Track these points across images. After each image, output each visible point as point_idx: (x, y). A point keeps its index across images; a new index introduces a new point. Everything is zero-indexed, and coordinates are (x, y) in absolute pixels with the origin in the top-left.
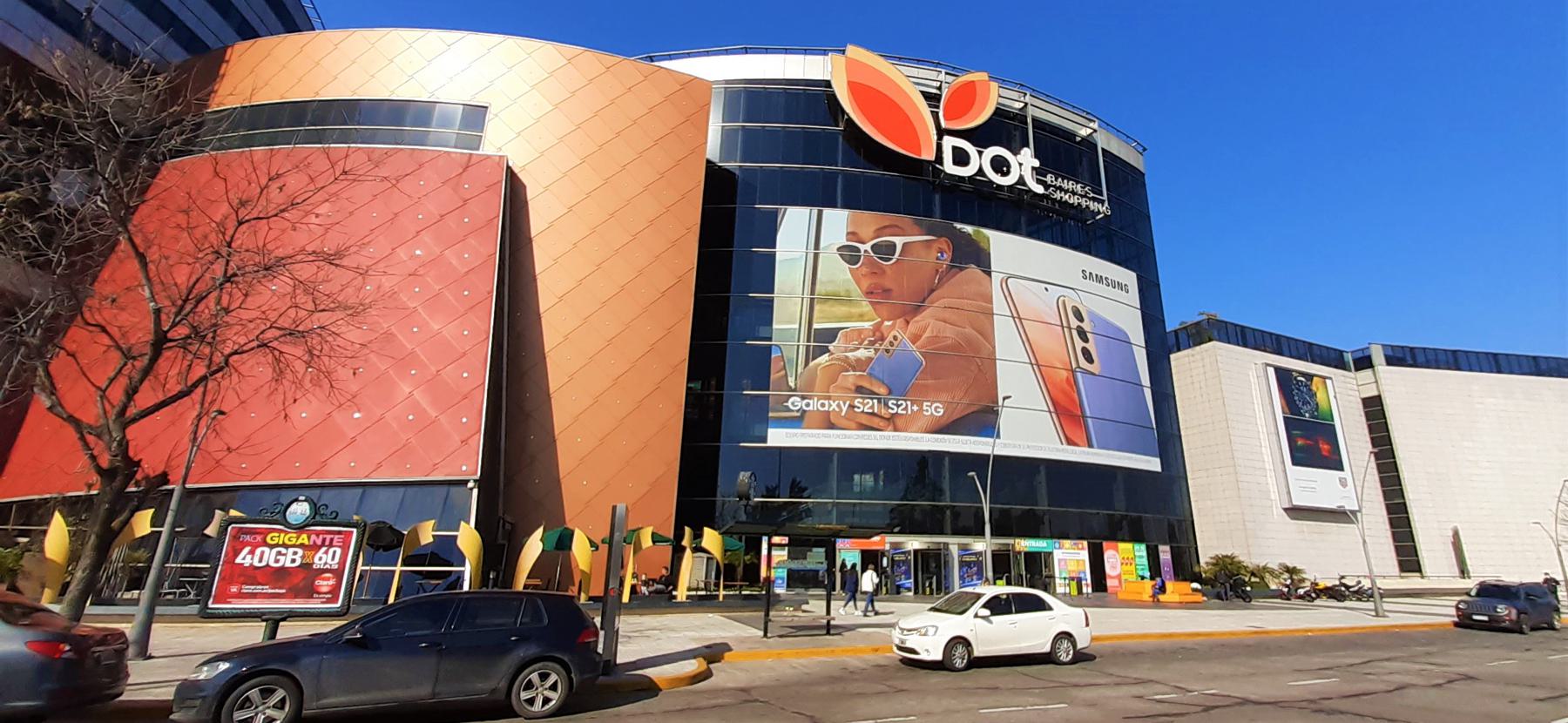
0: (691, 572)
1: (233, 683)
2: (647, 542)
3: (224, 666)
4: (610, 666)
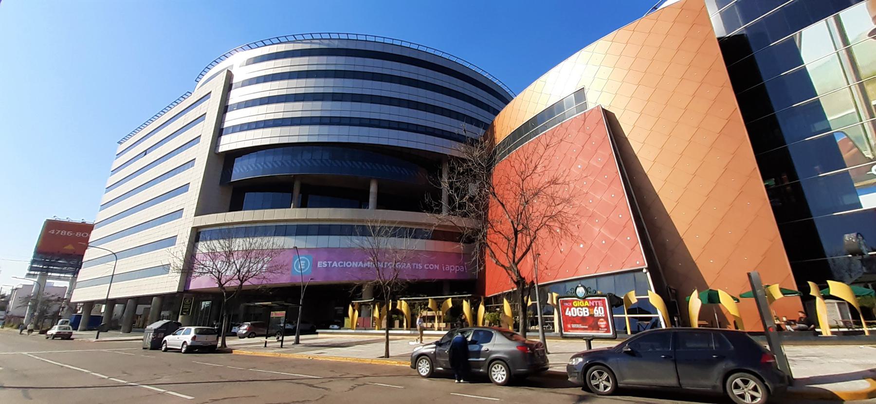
0: (827, 316)
1: (587, 368)
2: (778, 295)
3: (581, 360)
4: (791, 381)
